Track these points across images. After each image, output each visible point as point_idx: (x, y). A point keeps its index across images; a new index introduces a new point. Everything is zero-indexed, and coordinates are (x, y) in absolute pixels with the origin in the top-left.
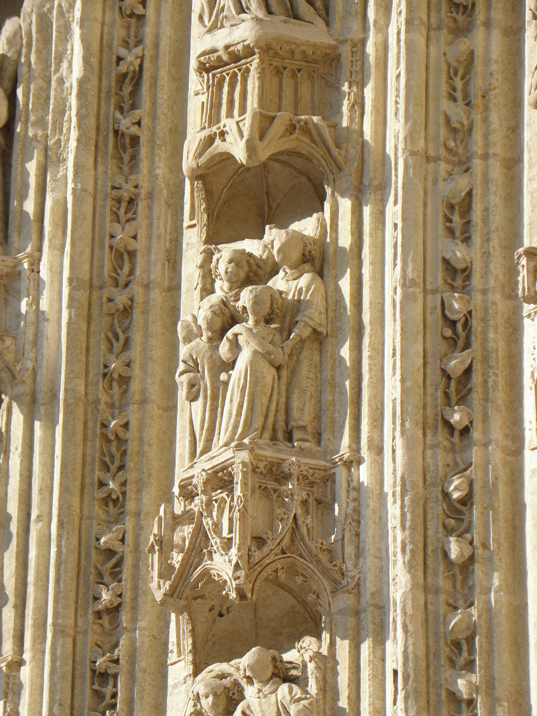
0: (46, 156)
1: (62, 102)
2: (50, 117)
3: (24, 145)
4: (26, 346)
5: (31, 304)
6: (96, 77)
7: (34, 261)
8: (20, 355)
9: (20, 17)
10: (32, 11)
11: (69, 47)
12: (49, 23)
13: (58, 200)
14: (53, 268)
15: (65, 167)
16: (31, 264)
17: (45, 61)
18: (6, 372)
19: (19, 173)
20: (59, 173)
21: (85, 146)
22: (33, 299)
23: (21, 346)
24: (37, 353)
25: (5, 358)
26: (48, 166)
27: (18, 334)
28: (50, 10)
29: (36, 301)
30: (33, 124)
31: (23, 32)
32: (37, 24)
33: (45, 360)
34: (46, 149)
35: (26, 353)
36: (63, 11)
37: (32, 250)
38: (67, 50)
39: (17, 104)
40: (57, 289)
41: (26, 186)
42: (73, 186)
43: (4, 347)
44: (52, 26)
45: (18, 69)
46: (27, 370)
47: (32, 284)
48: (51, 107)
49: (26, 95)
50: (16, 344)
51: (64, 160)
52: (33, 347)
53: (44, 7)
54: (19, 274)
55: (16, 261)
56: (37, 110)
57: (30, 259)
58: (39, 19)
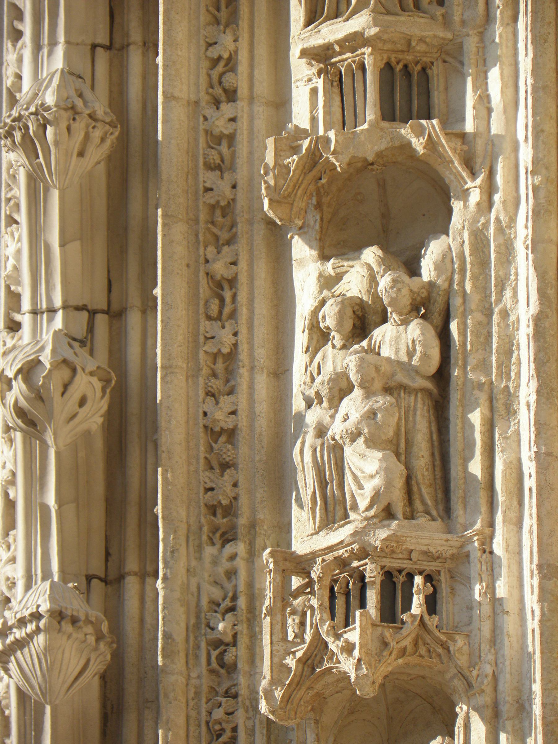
0: (492, 409)
1: (507, 340)
2: (494, 358)
3: (463, 395)
4: (483, 646)
5: (485, 593)
6: (555, 312)
7: (485, 538)
8: (475, 659)
9: (448, 235)
10: (464, 227)
11: (513, 271)
12: (485, 242)
13: (511, 462)
14: (510, 548)
15: (516, 421)
16: (482, 544)
17: (483, 288)
18: (460, 679)
19: (459, 430)
20: (509, 428)
21: (547, 399)
22: (487, 587)
23: (477, 645)
24: (496, 653)
25: (458, 662)
26: (496, 421)
27: (471, 631)
28: (486, 225)
29: (491, 588)
30: (473, 369)
31: (454, 255)
32: (471, 244)
33: (507, 663)
34: (491, 400)
35: (482, 654)
36: (502, 226)
37: (482, 526)
38: (510, 275)
39: (452, 344)
40: (516, 573)
41: (470, 445)
42: (536, 449)
43: (456, 648)
44: (489, 246)
45: (451, 301)
46: (486, 676)
47: (484, 568)
48: (494, 347)
49: (463, 332)
50: (469, 644)
51: (515, 412)
52: (491, 647)
53: (479, 222)
54: (468, 555)
55: (463, 540)
56: (477, 351)
57: (481, 537)
58: (473, 237)
